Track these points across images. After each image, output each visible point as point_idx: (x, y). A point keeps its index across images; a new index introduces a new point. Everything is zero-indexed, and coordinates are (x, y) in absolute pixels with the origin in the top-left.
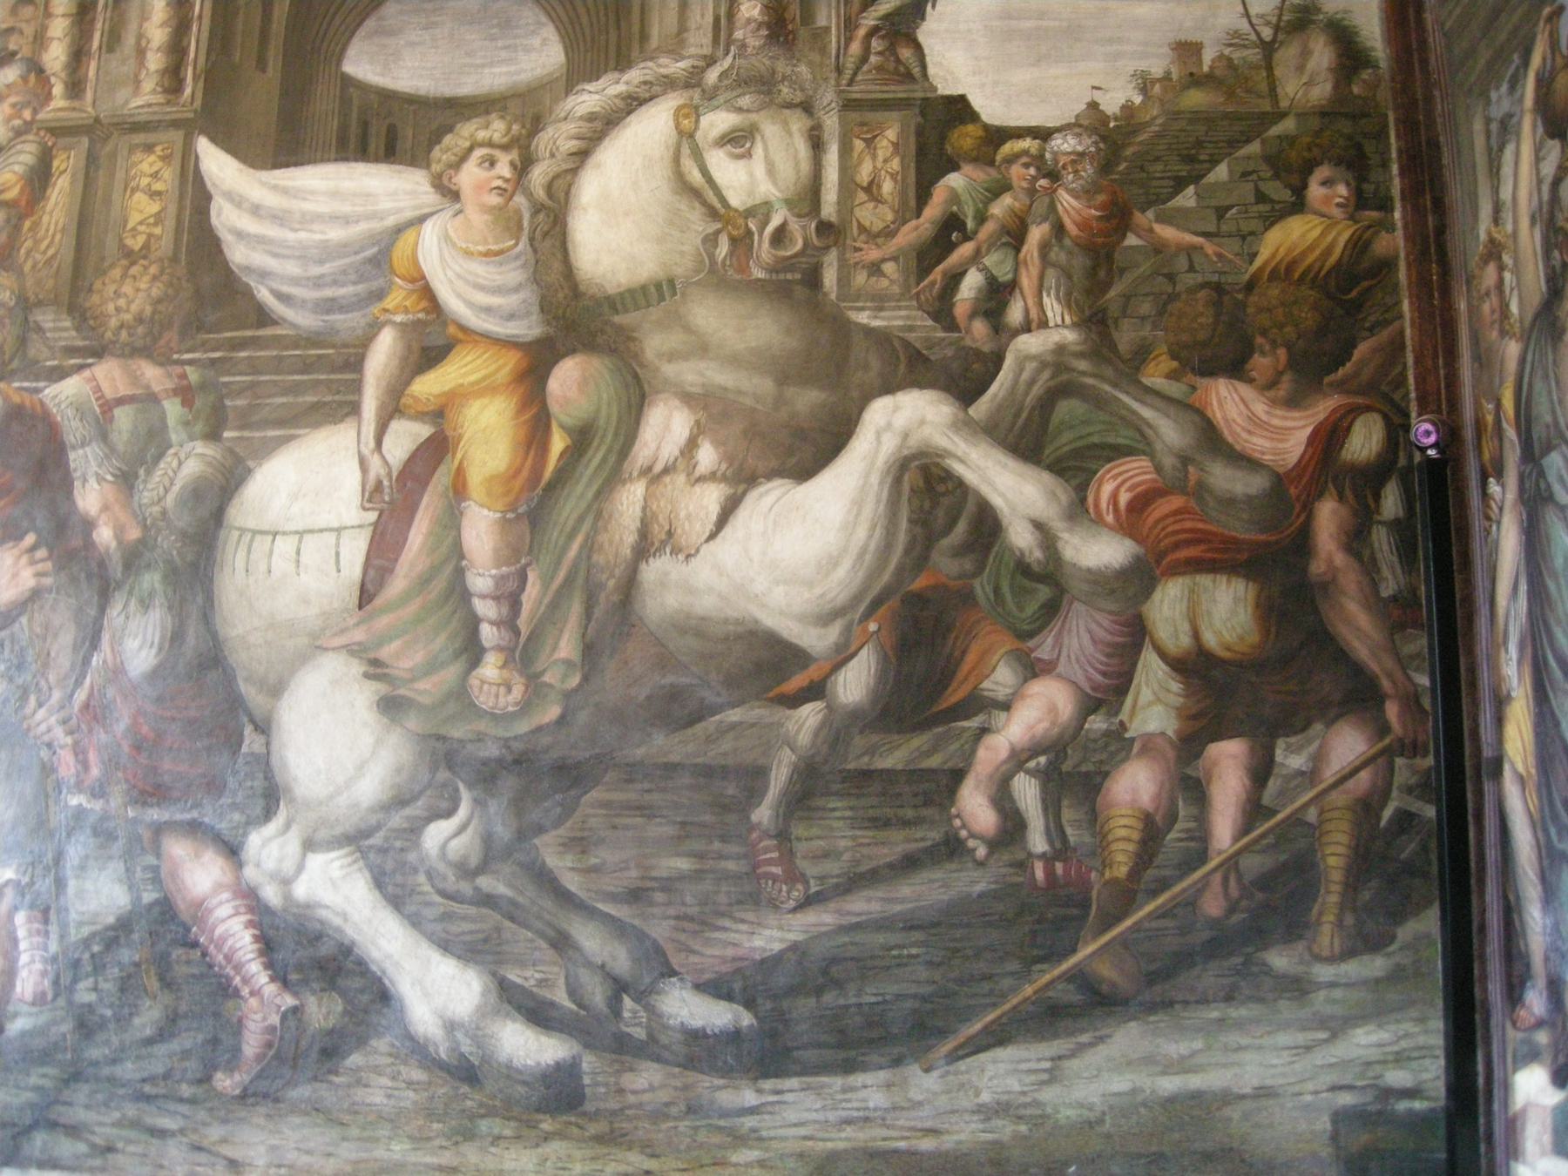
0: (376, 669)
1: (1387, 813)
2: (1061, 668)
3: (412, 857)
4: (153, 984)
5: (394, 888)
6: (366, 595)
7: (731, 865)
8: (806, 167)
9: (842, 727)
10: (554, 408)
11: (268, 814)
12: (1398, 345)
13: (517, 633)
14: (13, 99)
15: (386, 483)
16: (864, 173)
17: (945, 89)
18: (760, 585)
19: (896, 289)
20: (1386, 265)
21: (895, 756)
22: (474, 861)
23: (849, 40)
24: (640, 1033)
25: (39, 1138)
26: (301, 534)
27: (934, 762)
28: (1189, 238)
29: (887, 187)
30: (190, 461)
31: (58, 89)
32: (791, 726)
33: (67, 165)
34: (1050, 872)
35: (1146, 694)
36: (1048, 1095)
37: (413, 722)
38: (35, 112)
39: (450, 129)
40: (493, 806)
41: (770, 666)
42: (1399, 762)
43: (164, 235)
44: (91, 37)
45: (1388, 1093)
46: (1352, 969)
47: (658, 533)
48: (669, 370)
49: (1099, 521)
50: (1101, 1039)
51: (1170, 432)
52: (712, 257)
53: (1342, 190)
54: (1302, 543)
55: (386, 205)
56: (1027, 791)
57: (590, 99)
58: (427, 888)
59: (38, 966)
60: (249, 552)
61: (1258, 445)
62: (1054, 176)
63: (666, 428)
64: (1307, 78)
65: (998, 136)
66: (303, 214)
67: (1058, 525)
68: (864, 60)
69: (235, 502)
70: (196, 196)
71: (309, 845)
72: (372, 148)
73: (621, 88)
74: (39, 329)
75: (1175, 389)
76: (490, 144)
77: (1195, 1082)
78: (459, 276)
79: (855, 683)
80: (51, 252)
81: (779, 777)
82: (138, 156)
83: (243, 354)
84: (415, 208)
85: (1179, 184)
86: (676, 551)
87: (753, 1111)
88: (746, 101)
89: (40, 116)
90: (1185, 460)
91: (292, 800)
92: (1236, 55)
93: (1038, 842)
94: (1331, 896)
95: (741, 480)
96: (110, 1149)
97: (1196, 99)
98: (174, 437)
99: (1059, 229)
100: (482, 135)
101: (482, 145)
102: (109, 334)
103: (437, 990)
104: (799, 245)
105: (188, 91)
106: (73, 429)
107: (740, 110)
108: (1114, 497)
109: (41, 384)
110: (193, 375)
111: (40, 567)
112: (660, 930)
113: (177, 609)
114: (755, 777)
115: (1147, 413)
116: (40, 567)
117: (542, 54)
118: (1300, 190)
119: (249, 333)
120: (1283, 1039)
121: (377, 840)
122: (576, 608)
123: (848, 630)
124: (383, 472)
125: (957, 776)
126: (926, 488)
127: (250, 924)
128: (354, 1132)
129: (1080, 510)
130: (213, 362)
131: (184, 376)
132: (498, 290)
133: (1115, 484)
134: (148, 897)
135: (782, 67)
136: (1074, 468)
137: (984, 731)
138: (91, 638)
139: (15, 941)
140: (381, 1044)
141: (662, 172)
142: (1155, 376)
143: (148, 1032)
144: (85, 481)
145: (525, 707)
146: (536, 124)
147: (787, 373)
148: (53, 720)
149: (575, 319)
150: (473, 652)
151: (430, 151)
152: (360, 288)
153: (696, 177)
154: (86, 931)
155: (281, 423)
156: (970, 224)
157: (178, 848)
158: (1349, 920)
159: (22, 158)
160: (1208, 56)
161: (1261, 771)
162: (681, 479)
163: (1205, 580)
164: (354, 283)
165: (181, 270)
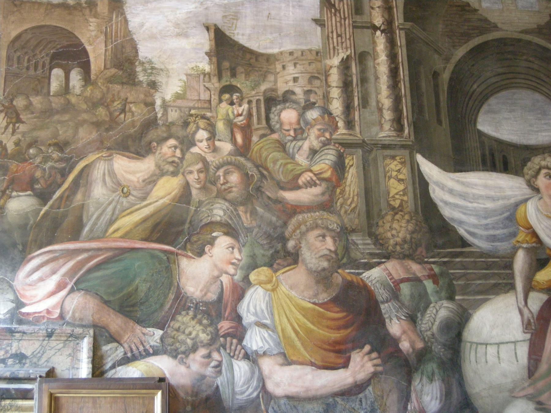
6: (532, 370)
14: (319, 127)
15: (532, 321)
26: (498, 344)
30: (440, 311)
31: (341, 124)
33: (353, 162)
38: (331, 134)
39: (529, 160)
44: (353, 100)
55: (509, 193)
60: (476, 353)
66: (474, 195)
69: (466, 329)
70: (421, 184)
72: (498, 166)
78: (547, 228)
80: (353, 205)
82: (388, 161)
83: (458, 260)
84: (523, 195)
89: (334, 137)
98: (432, 299)
100: (543, 163)
101: (544, 168)
102: (390, 248)
105: (406, 131)
106: (381, 294)
109: (361, 271)
110: (436, 269)
111: (375, 362)
113: (446, 382)
116: (375, 362)
119: (459, 250)
124: (530, 316)
130: (445, 263)
131: (432, 269)
138: (405, 398)
144: (391, 319)
151: (523, 169)
152: (505, 231)
159: (329, 157)
164: (503, 229)
165: (421, 217)
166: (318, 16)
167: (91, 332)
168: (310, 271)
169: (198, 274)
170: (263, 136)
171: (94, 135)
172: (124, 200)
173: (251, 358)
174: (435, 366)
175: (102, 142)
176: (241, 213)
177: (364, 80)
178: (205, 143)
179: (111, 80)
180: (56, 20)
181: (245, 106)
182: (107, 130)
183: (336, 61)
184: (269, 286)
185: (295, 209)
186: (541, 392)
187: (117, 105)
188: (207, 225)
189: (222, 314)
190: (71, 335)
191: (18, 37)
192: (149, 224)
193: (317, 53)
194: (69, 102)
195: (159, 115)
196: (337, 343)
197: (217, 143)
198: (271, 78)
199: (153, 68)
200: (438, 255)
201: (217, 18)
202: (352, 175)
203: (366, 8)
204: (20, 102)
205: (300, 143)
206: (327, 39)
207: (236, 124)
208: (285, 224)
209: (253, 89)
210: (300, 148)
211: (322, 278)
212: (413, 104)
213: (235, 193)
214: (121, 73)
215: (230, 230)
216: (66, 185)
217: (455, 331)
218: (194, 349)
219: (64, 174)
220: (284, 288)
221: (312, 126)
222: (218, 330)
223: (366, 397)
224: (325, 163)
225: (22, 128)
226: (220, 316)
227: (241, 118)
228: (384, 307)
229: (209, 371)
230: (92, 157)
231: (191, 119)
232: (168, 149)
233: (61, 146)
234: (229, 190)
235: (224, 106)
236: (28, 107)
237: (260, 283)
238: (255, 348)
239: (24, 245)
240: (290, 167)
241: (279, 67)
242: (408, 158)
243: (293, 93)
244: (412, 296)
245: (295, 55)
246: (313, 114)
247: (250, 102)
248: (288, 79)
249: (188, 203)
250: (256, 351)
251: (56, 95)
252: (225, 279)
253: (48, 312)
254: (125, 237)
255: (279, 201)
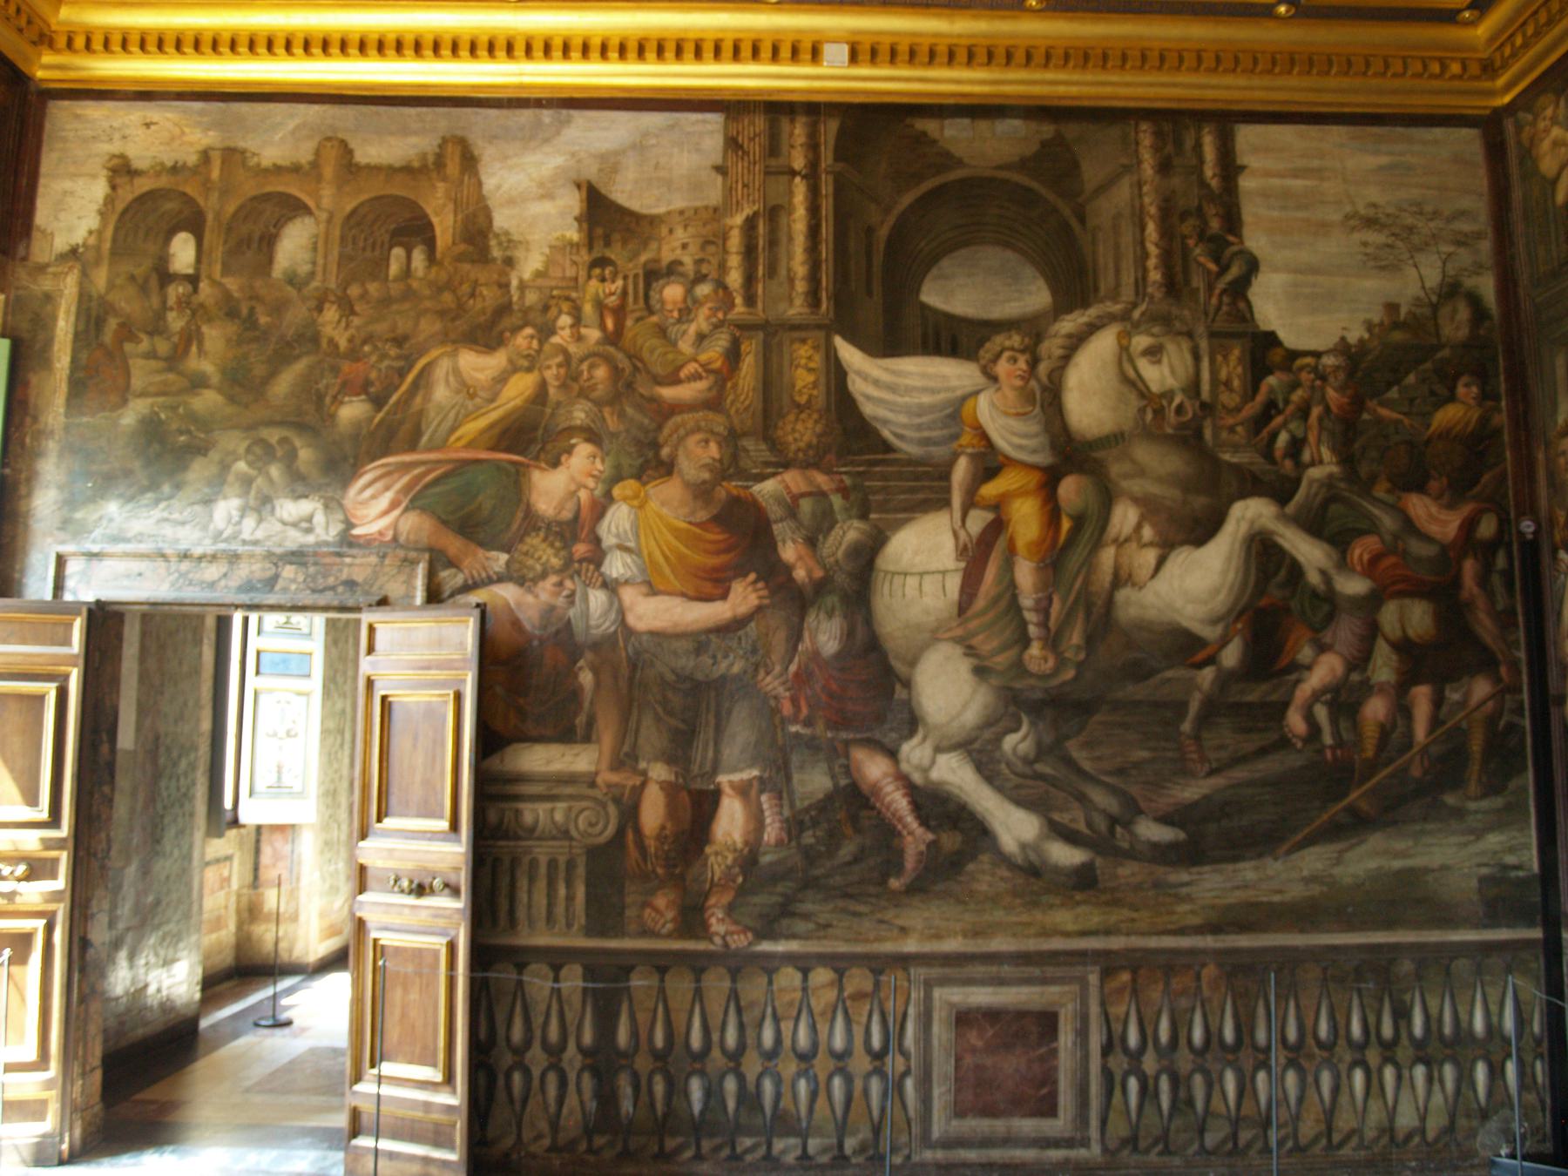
0: (970, 651)
1: (1502, 723)
2: (1337, 647)
3: (997, 754)
4: (849, 831)
5: (987, 768)
6: (963, 607)
7: (1170, 754)
8: (1191, 370)
9: (1226, 680)
10: (1063, 504)
11: (912, 733)
12: (1502, 478)
13: (1048, 629)
16: (1223, 375)
17: (1264, 327)
18: (1179, 604)
19: (1243, 441)
20: (1498, 432)
21: (1255, 694)
22: (1032, 756)
23: (1210, 296)
24: (1126, 845)
25: (785, 922)
26: (921, 574)
27: (1274, 697)
28: (1395, 415)
29: (1236, 383)
30: (850, 532)
31: (739, 300)
32: (1199, 680)
34: (1334, 754)
35: (1379, 662)
36: (1337, 871)
37: (994, 681)
38: (725, 314)
39: (988, 339)
40: (1041, 725)
41: (1185, 646)
42: (1508, 697)
43: (820, 395)
45: (1506, 868)
46: (1485, 804)
47: (1123, 574)
48: (1125, 484)
49: (1353, 570)
50: (1362, 842)
51: (1388, 522)
52: (1143, 420)
53: (1474, 389)
54: (1456, 582)
56: (1321, 713)
57: (1068, 324)
58: (1007, 771)
59: (777, 825)
61: (1433, 529)
62: (1323, 378)
63: (1125, 517)
64: (1456, 325)
65: (1294, 355)
66: (906, 387)
67: (1333, 572)
68: (1219, 308)
70: (837, 373)
71: (938, 749)
73: (1084, 319)
74: (747, 451)
75: (1390, 499)
76: (1012, 349)
77: (1409, 863)
79: (1231, 656)
81: (1194, 707)
82: (796, 346)
85: (1389, 385)
86: (1134, 585)
87: (1187, 884)
88: (1156, 330)
89: (729, 317)
90: (1396, 537)
91: (926, 724)
92: (1418, 311)
93: (1328, 739)
94: (1475, 767)
95: (1166, 547)
96: (828, 926)
97: (1398, 336)
99: (1327, 409)
100: (1008, 343)
103: (1015, 827)
104: (1190, 415)
105: (824, 306)
106: (774, 511)
107: (1153, 335)
108: (1361, 555)
110: (848, 481)
112: (1134, 790)
114: (1181, 708)
115: (1376, 512)
116: (762, 593)
117: (1036, 296)
118: (1452, 389)
119: (880, 457)
120: (1454, 839)
121: (976, 746)
122: (1081, 615)
123: (1226, 628)
125: (1286, 705)
126: (1263, 553)
127: (905, 795)
128: (972, 906)
129: (1343, 564)
130: (859, 474)
131: (842, 481)
132: (1026, 436)
133: (1361, 550)
134: (843, 782)
135: (1175, 311)
136: (1339, 541)
137: (1298, 681)
138: (796, 636)
139: (762, 811)
140: (985, 858)
141: (1112, 371)
142: (1380, 491)
143: (848, 858)
144: (784, 542)
145: (1056, 671)
146: (1038, 337)
147: (1187, 486)
148: (776, 683)
149: (1070, 454)
150: (1025, 641)
152: (945, 432)
153: (1131, 373)
154: (806, 803)
155: (905, 510)
156: (1281, 405)
157: (860, 755)
158: (1484, 779)
160: (1403, 311)
161: (1438, 701)
162: (1134, 545)
163: (1407, 601)
166: (719, 161)
167: (427, 556)
168: (687, 485)
169: (552, 489)
170: (638, 320)
171: (438, 326)
172: (470, 405)
173: (611, 586)
174: (836, 599)
175: (446, 335)
176: (607, 415)
177: (773, 243)
178: (567, 333)
179: (460, 258)
180: (397, 189)
181: (620, 283)
182: (453, 320)
183: (739, 220)
184: (636, 503)
185: (675, 408)
186: (974, 634)
187: (466, 288)
188: (565, 429)
189: (577, 534)
190: (405, 560)
191: (354, 212)
192: (496, 431)
193: (715, 210)
194: (409, 287)
195: (515, 299)
196: (716, 569)
197: (583, 331)
198: (654, 245)
199: (510, 241)
200: (852, 463)
201: (591, 172)
202: (749, 365)
203: (785, 148)
204: (354, 291)
205: (684, 327)
206: (729, 191)
207: (606, 306)
208: (660, 427)
209: (631, 260)
210: (684, 332)
211: (701, 492)
212: (836, 273)
213: (601, 391)
214: (471, 249)
215: (592, 436)
216: (404, 388)
217: (866, 557)
218: (544, 575)
219: (402, 374)
220: (653, 505)
221: (702, 304)
222: (571, 554)
223: (747, 635)
224: (714, 352)
225: (356, 321)
226: (575, 538)
227: (613, 298)
228: (777, 528)
229: (560, 601)
230: (434, 353)
231: (553, 302)
232: (524, 339)
233: (399, 341)
234: (593, 388)
235: (594, 283)
236: (364, 296)
237: (625, 499)
238: (615, 575)
239: (356, 457)
240: (670, 356)
241: (664, 231)
242: (823, 341)
243: (680, 263)
244: (814, 514)
245: (687, 215)
246: (704, 290)
247: (625, 278)
248: (676, 246)
249: (544, 404)
250: (616, 580)
251: (396, 280)
252: (583, 495)
253: (381, 533)
254: (470, 445)
255: (653, 400)
